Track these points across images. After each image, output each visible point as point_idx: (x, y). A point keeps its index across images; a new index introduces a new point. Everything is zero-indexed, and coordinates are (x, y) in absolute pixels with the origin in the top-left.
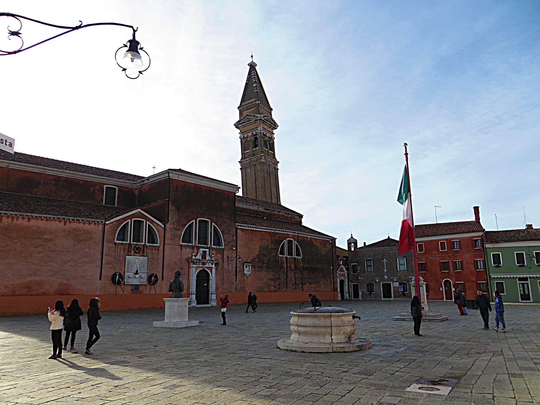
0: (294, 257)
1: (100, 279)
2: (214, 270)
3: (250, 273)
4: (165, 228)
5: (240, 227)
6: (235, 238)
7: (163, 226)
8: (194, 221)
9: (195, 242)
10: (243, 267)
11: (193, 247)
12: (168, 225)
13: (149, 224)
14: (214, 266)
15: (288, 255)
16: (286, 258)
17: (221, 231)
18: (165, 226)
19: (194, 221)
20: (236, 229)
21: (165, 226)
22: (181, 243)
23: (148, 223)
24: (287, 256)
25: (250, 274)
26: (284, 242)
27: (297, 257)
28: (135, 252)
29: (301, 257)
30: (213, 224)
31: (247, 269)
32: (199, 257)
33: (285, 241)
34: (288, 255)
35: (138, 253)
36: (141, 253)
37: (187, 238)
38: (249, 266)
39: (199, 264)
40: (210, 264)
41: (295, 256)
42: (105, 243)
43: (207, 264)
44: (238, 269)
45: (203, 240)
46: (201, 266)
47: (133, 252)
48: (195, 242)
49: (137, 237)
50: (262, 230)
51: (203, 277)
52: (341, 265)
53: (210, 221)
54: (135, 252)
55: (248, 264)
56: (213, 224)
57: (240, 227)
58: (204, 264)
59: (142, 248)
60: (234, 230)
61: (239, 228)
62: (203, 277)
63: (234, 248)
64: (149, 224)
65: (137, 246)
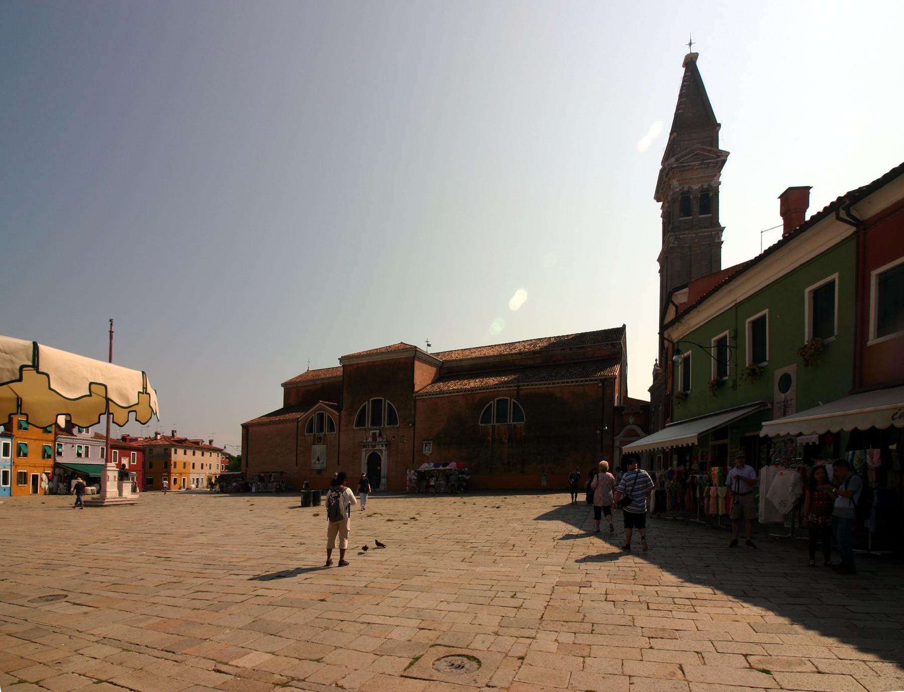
0: (509, 423)
1: (297, 466)
2: (384, 452)
3: (431, 452)
4: (340, 416)
5: (419, 398)
6: (413, 412)
7: (338, 414)
8: (367, 402)
9: (368, 424)
10: (423, 448)
11: (365, 430)
12: (343, 413)
13: (328, 415)
14: (384, 448)
15: (496, 422)
16: (493, 427)
17: (396, 407)
18: (340, 414)
19: (367, 402)
20: (415, 400)
21: (340, 414)
22: (354, 428)
23: (327, 413)
24: (495, 424)
25: (431, 454)
26: (491, 405)
27: (515, 423)
28: (318, 442)
29: (523, 423)
30: (387, 401)
31: (427, 448)
32: (370, 440)
33: (492, 402)
34: (496, 422)
35: (320, 442)
36: (322, 441)
37: (361, 422)
38: (430, 444)
39: (369, 448)
40: (381, 446)
41: (510, 422)
42: (299, 437)
43: (377, 446)
44: (416, 450)
45: (376, 421)
46: (371, 449)
47: (316, 441)
48: (368, 424)
49: (321, 429)
50: (451, 395)
51: (374, 460)
52: (629, 424)
53: (383, 399)
54: (318, 442)
55: (426, 442)
56: (387, 401)
57: (419, 398)
58: (374, 446)
59: (322, 436)
60: (413, 403)
61: (418, 399)
62: (374, 460)
63: (411, 425)
64: (328, 415)
65: (319, 436)
